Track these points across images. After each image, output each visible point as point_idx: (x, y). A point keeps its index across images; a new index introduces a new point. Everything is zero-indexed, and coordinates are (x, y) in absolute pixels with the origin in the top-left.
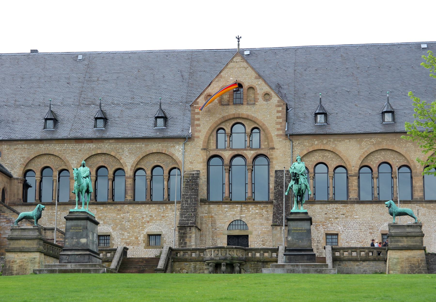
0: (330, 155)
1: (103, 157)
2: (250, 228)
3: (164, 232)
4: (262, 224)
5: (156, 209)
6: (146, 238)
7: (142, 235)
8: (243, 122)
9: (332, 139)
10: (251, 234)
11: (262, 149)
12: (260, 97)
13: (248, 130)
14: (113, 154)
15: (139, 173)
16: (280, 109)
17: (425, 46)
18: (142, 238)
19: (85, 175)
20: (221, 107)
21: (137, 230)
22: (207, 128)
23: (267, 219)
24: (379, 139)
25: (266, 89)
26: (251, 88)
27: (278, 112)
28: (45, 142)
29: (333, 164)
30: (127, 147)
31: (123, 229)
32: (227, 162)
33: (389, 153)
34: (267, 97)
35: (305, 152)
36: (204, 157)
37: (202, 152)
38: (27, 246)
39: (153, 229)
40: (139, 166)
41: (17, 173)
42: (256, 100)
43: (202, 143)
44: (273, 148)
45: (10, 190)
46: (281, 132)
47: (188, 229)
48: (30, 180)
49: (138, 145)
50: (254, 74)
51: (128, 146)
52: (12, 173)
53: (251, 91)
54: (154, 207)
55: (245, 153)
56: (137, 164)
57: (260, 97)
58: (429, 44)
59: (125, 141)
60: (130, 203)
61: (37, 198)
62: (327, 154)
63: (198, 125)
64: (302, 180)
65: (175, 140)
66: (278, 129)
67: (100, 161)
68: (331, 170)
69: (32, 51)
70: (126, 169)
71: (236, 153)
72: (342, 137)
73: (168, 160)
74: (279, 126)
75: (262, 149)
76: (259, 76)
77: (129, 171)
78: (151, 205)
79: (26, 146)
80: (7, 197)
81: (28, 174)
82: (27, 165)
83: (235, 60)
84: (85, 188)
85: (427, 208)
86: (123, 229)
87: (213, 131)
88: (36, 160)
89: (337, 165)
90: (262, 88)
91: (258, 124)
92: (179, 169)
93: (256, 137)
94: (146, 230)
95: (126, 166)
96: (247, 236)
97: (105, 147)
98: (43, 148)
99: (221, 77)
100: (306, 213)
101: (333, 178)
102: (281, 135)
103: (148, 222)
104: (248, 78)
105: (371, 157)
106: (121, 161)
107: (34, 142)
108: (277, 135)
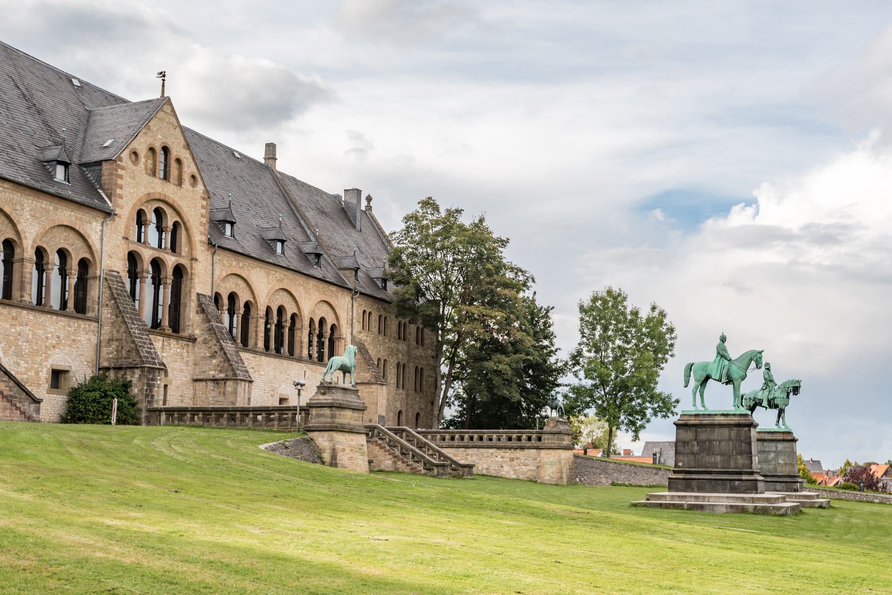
4: (181, 371)
5: (64, 327)
6: (49, 376)
9: (249, 262)
11: (183, 257)
33: (285, 294)
35: (224, 274)
37: (123, 241)
43: (123, 227)
44: (196, 260)
46: (204, 239)
47: (157, 374)
50: (183, 142)
51: (30, 201)
57: (186, 178)
59: (28, 192)
62: (240, 282)
63: (121, 197)
65: (94, 213)
66: (202, 233)
72: (256, 263)
74: (202, 229)
75: (183, 257)
76: (188, 146)
78: (59, 318)
85: (311, 369)
99: (149, 129)
102: (204, 243)
103: (54, 347)
108: (201, 242)
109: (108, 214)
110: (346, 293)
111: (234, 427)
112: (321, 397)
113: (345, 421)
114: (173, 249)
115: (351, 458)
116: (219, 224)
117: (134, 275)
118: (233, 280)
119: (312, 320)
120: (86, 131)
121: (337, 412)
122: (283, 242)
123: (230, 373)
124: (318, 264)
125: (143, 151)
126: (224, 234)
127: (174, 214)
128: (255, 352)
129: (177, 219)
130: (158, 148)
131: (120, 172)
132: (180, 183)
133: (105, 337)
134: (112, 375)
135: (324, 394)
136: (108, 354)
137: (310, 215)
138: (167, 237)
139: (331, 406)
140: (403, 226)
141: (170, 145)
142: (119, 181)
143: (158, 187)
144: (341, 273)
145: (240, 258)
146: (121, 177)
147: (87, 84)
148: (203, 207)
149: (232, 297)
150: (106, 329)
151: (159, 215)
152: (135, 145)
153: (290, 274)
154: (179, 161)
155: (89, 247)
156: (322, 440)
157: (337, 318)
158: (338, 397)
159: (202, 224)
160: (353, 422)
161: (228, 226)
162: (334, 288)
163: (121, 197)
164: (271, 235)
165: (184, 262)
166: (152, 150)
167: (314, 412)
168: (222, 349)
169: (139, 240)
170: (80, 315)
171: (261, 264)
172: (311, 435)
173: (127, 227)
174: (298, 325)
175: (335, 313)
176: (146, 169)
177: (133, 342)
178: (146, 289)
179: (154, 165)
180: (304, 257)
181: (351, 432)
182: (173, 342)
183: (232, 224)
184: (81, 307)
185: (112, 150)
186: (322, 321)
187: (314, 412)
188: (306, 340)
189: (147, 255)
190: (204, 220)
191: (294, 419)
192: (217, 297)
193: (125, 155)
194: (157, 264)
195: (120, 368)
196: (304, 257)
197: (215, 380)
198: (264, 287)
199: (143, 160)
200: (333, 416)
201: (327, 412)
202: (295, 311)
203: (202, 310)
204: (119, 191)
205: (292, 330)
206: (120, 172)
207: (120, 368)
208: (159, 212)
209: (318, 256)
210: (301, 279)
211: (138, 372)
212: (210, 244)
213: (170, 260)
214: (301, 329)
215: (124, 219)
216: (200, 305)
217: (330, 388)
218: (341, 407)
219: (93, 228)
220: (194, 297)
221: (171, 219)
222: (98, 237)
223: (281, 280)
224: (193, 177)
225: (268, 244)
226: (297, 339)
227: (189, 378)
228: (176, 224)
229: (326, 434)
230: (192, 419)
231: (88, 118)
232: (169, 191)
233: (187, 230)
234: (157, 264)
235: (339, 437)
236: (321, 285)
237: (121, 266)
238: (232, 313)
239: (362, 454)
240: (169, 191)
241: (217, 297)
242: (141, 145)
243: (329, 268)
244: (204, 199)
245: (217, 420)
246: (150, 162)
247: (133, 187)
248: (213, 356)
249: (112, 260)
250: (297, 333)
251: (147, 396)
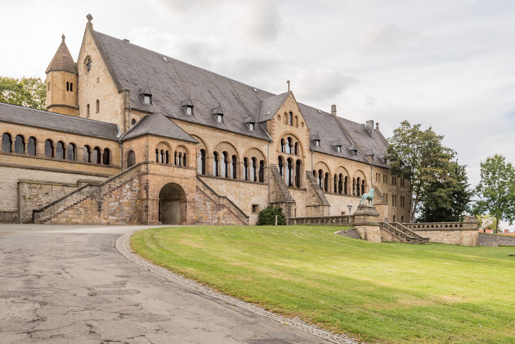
1: (226, 145)
4: (301, 203)
9: (326, 156)
14: (233, 144)
18: (250, 207)
20: (284, 125)
21: (247, 201)
23: (303, 200)
28: (193, 125)
33: (342, 168)
35: (317, 162)
46: (308, 148)
50: (298, 109)
57: (300, 123)
62: (323, 165)
63: (274, 134)
65: (265, 142)
66: (307, 146)
67: (226, 148)
72: (329, 156)
73: (260, 154)
74: (307, 144)
76: (300, 110)
91: (298, 140)
97: (229, 138)
107: (186, 123)
109: (270, 142)
110: (368, 166)
111: (323, 225)
112: (360, 211)
113: (371, 221)
114: (296, 153)
115: (373, 237)
116: (313, 142)
117: (281, 166)
118: (320, 164)
119: (354, 179)
120: (260, 109)
121: (367, 217)
122: (340, 146)
123: (321, 203)
124: (356, 155)
125: (282, 115)
126: (316, 145)
127: (295, 139)
128: (330, 194)
129: (297, 141)
131: (274, 124)
132: (297, 126)
133: (271, 191)
134: (274, 206)
135: (361, 210)
136: (273, 198)
137: (352, 134)
138: (293, 149)
139: (364, 215)
140: (393, 135)
142: (274, 128)
143: (289, 129)
144: (366, 158)
145: (323, 155)
146: (274, 126)
147: (260, 90)
148: (307, 135)
149: (320, 171)
150: (272, 188)
151: (290, 140)
153: (344, 160)
154: (296, 117)
155: (264, 155)
156: (361, 229)
157: (365, 177)
158: (367, 211)
159: (307, 142)
160: (373, 221)
161: (317, 142)
162: (363, 164)
163: (274, 134)
164: (336, 144)
165: (300, 158)
166: (286, 114)
167: (356, 217)
168: (317, 193)
169: (282, 151)
170: (261, 183)
171: (332, 157)
172: (356, 227)
173: (277, 146)
174: (348, 181)
175: (364, 175)
177: (282, 192)
178: (286, 171)
179: (287, 120)
180: (350, 152)
181: (373, 225)
182: (297, 191)
183: (319, 141)
184: (262, 180)
185: (270, 116)
186: (358, 179)
187: (356, 217)
188: (352, 187)
189: (286, 157)
190: (308, 140)
191: (348, 221)
192: (314, 172)
193: (275, 117)
194: (289, 160)
195: (277, 203)
196: (350, 152)
197: (315, 206)
198: (334, 166)
200: (365, 219)
201: (362, 217)
202: (347, 175)
203: (308, 177)
204: (274, 132)
205: (346, 183)
206: (274, 124)
207: (277, 203)
208: (289, 139)
209: (356, 151)
210: (349, 161)
211: (284, 204)
212: (311, 150)
213: (295, 158)
214: (349, 183)
215: (276, 143)
216: (307, 176)
217: (363, 207)
218: (368, 215)
219: (264, 147)
220: (305, 172)
221: (294, 141)
222: (267, 151)
223: (340, 163)
224: (302, 123)
225: (334, 148)
226: (348, 187)
227: (304, 206)
228: (296, 144)
229: (362, 227)
230: (307, 222)
231: (260, 104)
232: (293, 130)
233: (301, 145)
234: (289, 160)
235: (368, 228)
236: (358, 163)
237: (276, 162)
238: (320, 178)
239: (378, 235)
240: (293, 130)
241: (314, 172)
242: (281, 112)
243: (361, 156)
244: (307, 132)
245: (316, 222)
246: (285, 119)
247: (279, 129)
248: (313, 196)
249: (272, 161)
250: (348, 185)
251: (288, 214)
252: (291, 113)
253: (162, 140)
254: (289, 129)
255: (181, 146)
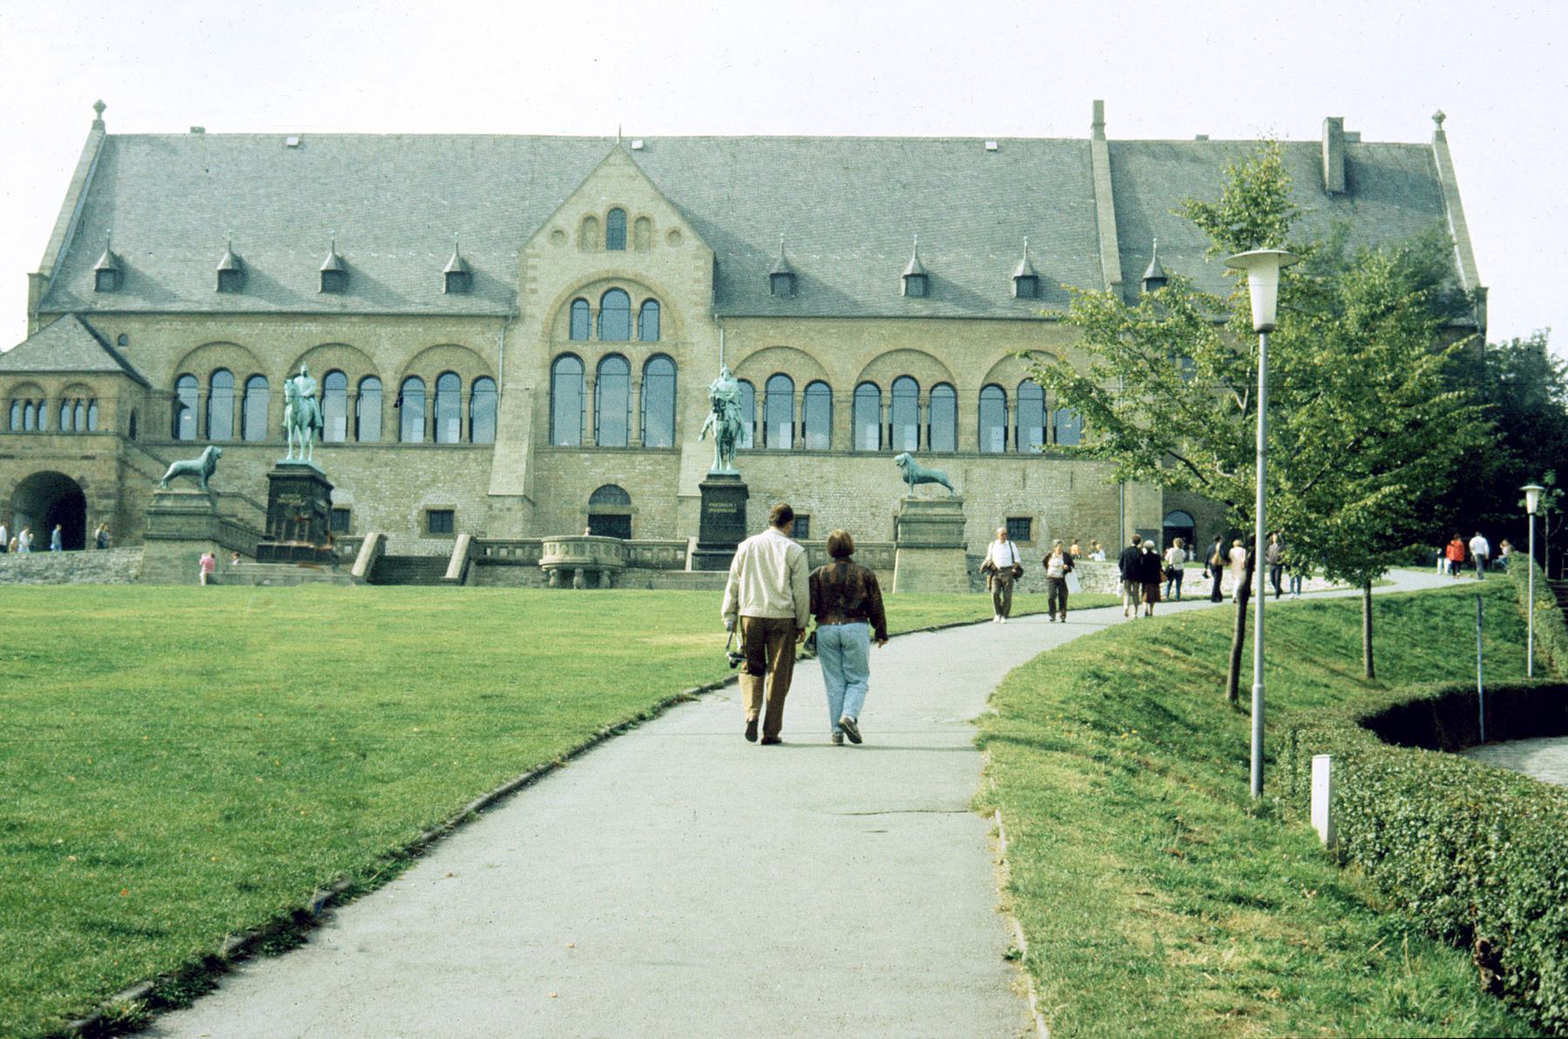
0: (799, 359)
1: (338, 352)
2: (635, 502)
3: (459, 507)
7: (415, 513)
8: (627, 289)
10: (637, 511)
12: (661, 237)
13: (636, 305)
15: (411, 385)
16: (701, 263)
17: (993, 146)
18: (415, 514)
19: (307, 393)
22: (553, 297)
24: (896, 326)
25: (675, 221)
26: (643, 218)
27: (697, 268)
29: (802, 378)
30: (385, 331)
31: (376, 495)
32: (591, 367)
33: (914, 357)
34: (675, 237)
35: (749, 352)
36: (543, 355)
38: (187, 528)
39: (437, 499)
40: (410, 372)
41: (159, 379)
42: (650, 244)
45: (147, 413)
46: (702, 310)
48: (187, 394)
49: (409, 328)
52: (150, 380)
53: (643, 225)
54: (441, 456)
55: (627, 350)
56: (407, 368)
57: (661, 237)
58: (998, 141)
60: (391, 447)
61: (202, 432)
62: (792, 355)
64: (730, 411)
67: (332, 358)
68: (800, 388)
69: (193, 130)
70: (383, 376)
71: (610, 349)
73: (472, 362)
77: (391, 383)
79: (178, 325)
80: (140, 427)
81: (183, 382)
82: (181, 364)
83: (611, 159)
84: (307, 420)
86: (376, 495)
87: (564, 304)
88: (200, 353)
89: (814, 378)
90: (665, 219)
92: (493, 380)
93: (649, 315)
94: (422, 505)
95: (384, 370)
96: (627, 518)
98: (214, 329)
100: (737, 477)
101: (804, 404)
104: (638, 201)
105: (879, 366)
106: (375, 361)
130: (601, 212)
141: (622, 201)
143: (605, 262)
146: (534, 267)
152: (559, 221)
166: (590, 219)
176: (582, 244)
199: (573, 236)
252: (617, 213)
253: (22, 379)
254: (605, 262)
255: (79, 385)
